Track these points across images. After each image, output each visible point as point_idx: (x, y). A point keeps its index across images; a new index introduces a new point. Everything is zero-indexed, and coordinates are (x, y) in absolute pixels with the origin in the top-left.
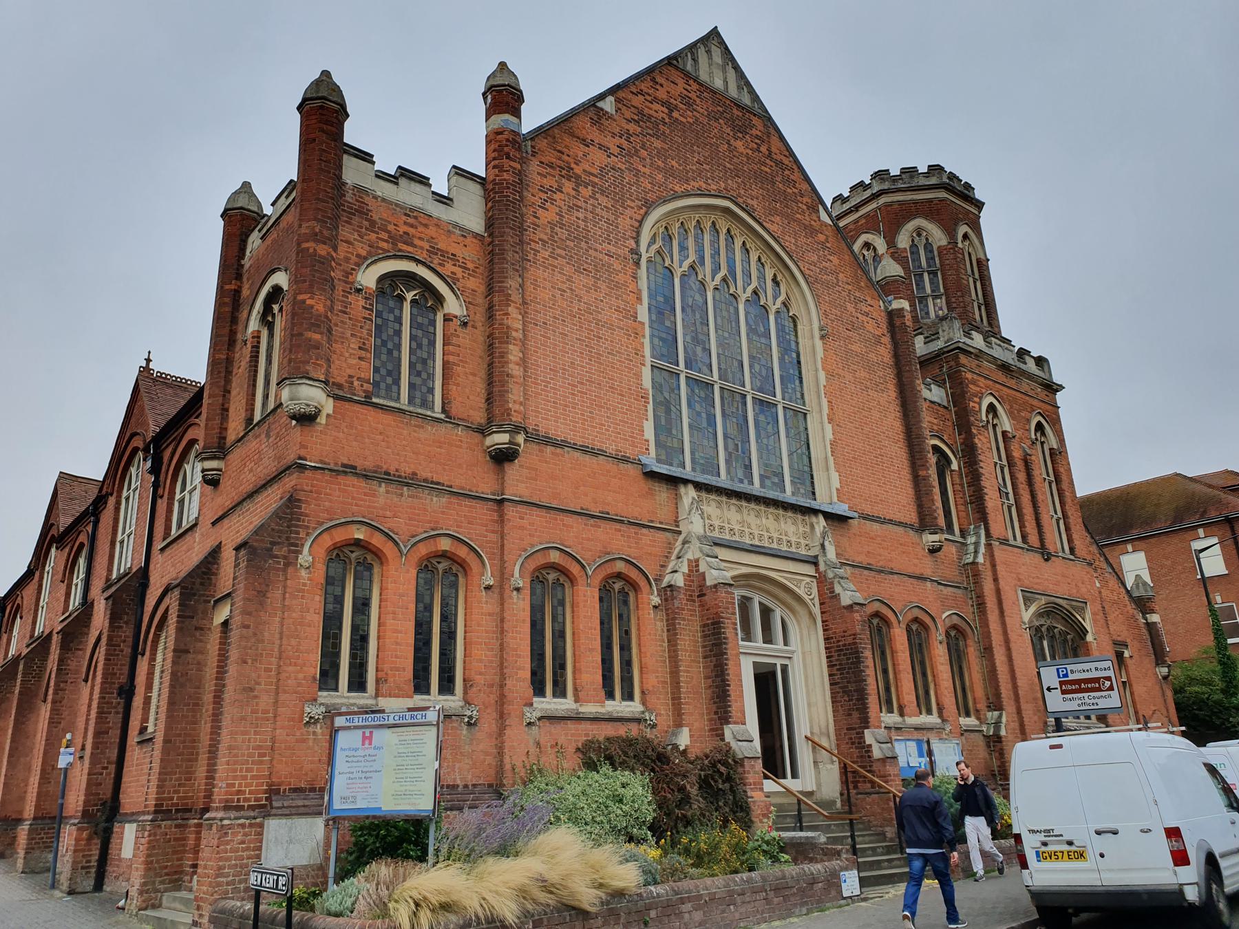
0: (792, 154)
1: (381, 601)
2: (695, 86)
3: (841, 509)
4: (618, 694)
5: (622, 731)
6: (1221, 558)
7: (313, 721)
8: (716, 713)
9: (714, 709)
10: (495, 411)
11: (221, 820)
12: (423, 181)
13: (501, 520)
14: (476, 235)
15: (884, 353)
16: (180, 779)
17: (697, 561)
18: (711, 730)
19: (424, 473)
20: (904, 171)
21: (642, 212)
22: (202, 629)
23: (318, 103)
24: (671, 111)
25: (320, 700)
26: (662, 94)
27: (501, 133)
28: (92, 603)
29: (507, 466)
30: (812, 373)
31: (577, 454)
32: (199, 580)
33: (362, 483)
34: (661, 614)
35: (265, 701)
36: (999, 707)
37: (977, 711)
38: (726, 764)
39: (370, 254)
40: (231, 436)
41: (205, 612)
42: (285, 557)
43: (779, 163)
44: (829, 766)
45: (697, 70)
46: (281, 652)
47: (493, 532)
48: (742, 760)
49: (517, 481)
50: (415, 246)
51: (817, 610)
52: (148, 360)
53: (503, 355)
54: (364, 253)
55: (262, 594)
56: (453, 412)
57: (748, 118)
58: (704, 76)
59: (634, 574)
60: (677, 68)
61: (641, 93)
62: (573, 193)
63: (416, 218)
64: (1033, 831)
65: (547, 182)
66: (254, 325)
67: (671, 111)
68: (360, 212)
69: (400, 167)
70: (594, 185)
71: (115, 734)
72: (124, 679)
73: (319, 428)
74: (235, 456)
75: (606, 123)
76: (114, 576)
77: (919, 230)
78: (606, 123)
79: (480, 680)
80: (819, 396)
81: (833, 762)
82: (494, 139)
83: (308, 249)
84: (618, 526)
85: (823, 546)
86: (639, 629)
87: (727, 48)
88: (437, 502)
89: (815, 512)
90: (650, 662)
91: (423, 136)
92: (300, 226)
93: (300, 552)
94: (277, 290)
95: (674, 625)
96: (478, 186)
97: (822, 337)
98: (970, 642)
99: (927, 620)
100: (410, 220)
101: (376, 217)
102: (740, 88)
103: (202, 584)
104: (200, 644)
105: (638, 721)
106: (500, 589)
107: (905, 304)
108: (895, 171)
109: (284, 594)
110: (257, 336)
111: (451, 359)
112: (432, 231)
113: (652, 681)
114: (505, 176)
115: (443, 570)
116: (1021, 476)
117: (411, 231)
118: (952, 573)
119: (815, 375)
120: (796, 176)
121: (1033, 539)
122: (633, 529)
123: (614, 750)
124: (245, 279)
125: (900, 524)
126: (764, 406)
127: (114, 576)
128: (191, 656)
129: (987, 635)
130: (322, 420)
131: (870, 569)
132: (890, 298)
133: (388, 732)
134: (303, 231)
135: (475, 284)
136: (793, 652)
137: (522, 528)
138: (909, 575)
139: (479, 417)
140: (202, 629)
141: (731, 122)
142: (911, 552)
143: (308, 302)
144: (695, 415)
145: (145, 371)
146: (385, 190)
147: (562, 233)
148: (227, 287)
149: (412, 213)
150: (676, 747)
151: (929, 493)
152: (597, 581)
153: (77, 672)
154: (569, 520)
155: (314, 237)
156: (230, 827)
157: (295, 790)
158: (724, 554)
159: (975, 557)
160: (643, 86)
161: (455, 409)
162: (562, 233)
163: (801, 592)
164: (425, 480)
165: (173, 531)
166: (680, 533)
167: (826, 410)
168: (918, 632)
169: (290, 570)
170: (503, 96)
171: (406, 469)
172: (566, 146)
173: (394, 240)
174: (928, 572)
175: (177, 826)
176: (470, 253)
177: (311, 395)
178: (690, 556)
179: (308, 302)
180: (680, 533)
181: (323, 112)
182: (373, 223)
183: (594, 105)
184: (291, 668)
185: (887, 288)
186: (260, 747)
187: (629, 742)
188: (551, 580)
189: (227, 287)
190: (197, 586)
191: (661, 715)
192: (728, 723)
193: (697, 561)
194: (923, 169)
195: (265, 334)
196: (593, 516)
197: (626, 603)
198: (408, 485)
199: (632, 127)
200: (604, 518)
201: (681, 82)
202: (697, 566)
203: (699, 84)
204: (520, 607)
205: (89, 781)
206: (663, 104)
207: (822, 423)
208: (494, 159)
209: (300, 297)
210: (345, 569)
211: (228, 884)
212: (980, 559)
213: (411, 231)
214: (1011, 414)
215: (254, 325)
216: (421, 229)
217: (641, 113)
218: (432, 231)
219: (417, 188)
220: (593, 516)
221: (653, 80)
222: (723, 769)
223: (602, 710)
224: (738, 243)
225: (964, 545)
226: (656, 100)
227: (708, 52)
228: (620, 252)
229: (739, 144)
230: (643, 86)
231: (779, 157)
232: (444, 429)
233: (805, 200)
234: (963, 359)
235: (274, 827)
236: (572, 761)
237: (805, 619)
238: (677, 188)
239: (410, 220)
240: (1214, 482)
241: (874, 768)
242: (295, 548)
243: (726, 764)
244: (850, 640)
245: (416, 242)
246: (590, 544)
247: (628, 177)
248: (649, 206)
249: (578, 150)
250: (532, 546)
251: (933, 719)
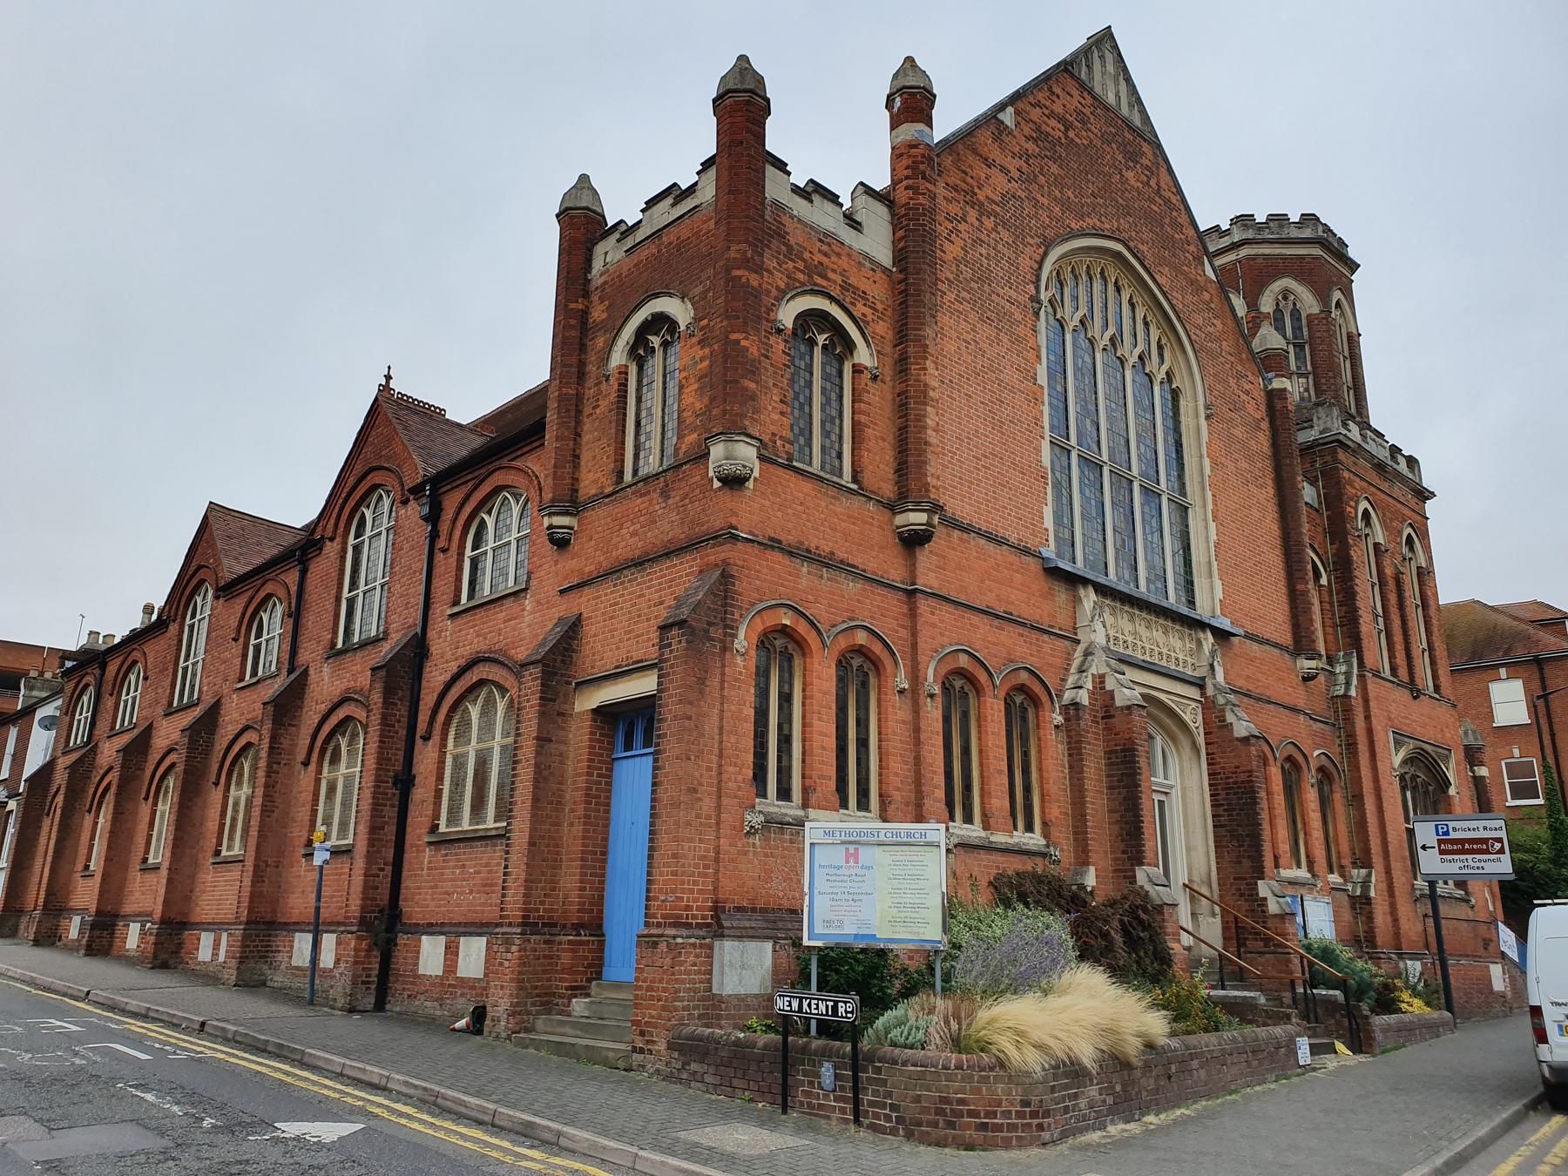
0: (1180, 192)
1: (804, 697)
2: (1089, 100)
3: (1225, 623)
4: (1020, 825)
5: (1027, 865)
6: (1524, 704)
7: (752, 832)
8: (1124, 852)
9: (1122, 847)
10: (909, 483)
11: (674, 937)
12: (833, 198)
13: (913, 614)
14: (885, 270)
15: (1262, 442)
16: (543, 888)
17: (1102, 677)
18: (1115, 871)
19: (841, 555)
20: (1272, 218)
21: (1041, 251)
22: (563, 714)
23: (745, 96)
24: (1067, 129)
25: (758, 808)
26: (1058, 108)
27: (915, 146)
28: (305, 673)
29: (917, 549)
30: (1195, 460)
31: (982, 542)
32: (560, 658)
33: (786, 560)
34: (1063, 735)
35: (708, 804)
36: (1367, 864)
37: (1342, 867)
38: (1145, 910)
39: (789, 288)
40: (587, 488)
41: (566, 695)
42: (721, 641)
43: (1167, 201)
44: (1211, 920)
45: (1091, 79)
46: (721, 751)
47: (904, 627)
48: (1161, 906)
49: (929, 570)
50: (828, 279)
51: (1201, 740)
52: (388, 377)
53: (921, 418)
54: (782, 286)
55: (702, 681)
56: (866, 483)
57: (1137, 141)
58: (1098, 89)
59: (1037, 688)
60: (1072, 76)
61: (1037, 105)
62: (977, 223)
63: (829, 245)
64: (1558, 1004)
65: (954, 209)
66: (618, 357)
67: (1067, 129)
68: (778, 234)
69: (812, 181)
70: (996, 215)
71: (390, 831)
72: (399, 767)
73: (748, 493)
74: (599, 517)
75: (1007, 139)
76: (356, 640)
77: (1286, 294)
78: (1007, 139)
79: (896, 795)
80: (1203, 489)
81: (1214, 915)
82: (897, 154)
83: (740, 277)
84: (1020, 630)
85: (1212, 666)
86: (1039, 752)
87: (1120, 55)
88: (853, 587)
90: (1053, 788)
91: (833, 147)
92: (729, 248)
93: (735, 636)
94: (660, 322)
95: (1080, 749)
96: (885, 210)
97: (1208, 417)
98: (1336, 787)
99: (1300, 759)
100: (825, 248)
101: (792, 242)
102: (1131, 105)
103: (563, 662)
104: (562, 733)
105: (1044, 855)
106: (913, 693)
108: (1261, 218)
109: (723, 681)
110: (623, 372)
111: (863, 418)
112: (844, 262)
113: (1054, 812)
114: (921, 200)
115: (859, 670)
117: (825, 260)
118: (1320, 706)
120: (1183, 219)
122: (1034, 635)
123: (1029, 887)
124: (595, 298)
125: (1276, 645)
126: (1151, 494)
127: (356, 640)
128: (553, 746)
129: (1358, 781)
130: (750, 484)
131: (1250, 696)
132: (1270, 375)
133: (878, 851)
134: (732, 254)
135: (883, 328)
136: (1171, 787)
137: (934, 625)
138: (1277, 707)
139: (888, 490)
140: (563, 714)
141: (1123, 145)
142: (1281, 676)
143: (743, 343)
144: (1085, 500)
145: (385, 389)
146: (799, 206)
147: (967, 273)
148: (572, 306)
149: (826, 237)
150: (1082, 887)
151: (1308, 611)
152: (1002, 694)
153: (291, 752)
154: (976, 619)
155: (745, 263)
156: (683, 946)
157: (739, 909)
159: (1348, 688)
160: (1040, 96)
161: (868, 479)
162: (967, 273)
163: (1187, 718)
164: (842, 562)
165: (464, 599)
166: (1078, 642)
167: (1210, 506)
168: (1292, 768)
169: (728, 655)
170: (911, 100)
171: (826, 548)
172: (970, 167)
173: (810, 270)
174: (1301, 704)
175: (546, 942)
176: (878, 291)
177: (746, 453)
178: (1093, 670)
179: (743, 343)
180: (1078, 642)
181: (742, 106)
182: (790, 248)
183: (995, 117)
184: (731, 769)
185: (1270, 362)
186: (703, 858)
187: (1038, 879)
189: (572, 306)
190: (558, 664)
191: (1063, 851)
192: (1142, 864)
193: (1102, 677)
194: (1295, 218)
195: (633, 370)
196: (998, 617)
197: (1024, 719)
198: (827, 566)
199: (1030, 146)
200: (1008, 619)
201: (1075, 92)
202: (1103, 682)
203: (1094, 98)
204: (933, 713)
205: (365, 882)
206: (1061, 119)
207: (1206, 520)
208: (907, 178)
209: (734, 336)
210: (769, 658)
211: (684, 1009)
212: (1353, 693)
213: (825, 260)
215: (618, 357)
216: (834, 259)
217: (1038, 129)
218: (844, 262)
219: (829, 206)
220: (998, 617)
221: (1050, 89)
222: (1143, 916)
223: (1010, 841)
224: (1125, 297)
225: (1333, 674)
226: (1052, 115)
227: (1102, 57)
228: (1021, 298)
229: (1130, 175)
230: (1040, 96)
231: (1168, 194)
232: (857, 501)
233: (1192, 248)
234: (1341, 455)
235: (728, 950)
236: (984, 897)
237: (1187, 750)
238: (1073, 225)
239: (825, 248)
240: (1521, 614)
241: (1269, 925)
242: (730, 630)
243: (1145, 910)
244: (1243, 777)
245: (831, 275)
246: (1000, 648)
247: (1028, 208)
248: (1048, 245)
249: (981, 171)
250: (943, 647)
251: (1302, 873)
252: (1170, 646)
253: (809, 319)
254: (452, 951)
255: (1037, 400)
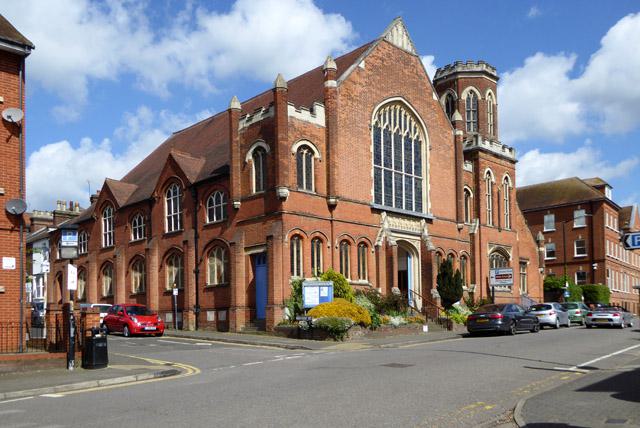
3: (430, 216)
26: (381, 56)
43: (420, 76)
51: (419, 251)
77: (471, 91)
88: (315, 220)
89: (421, 218)
107: (461, 133)
116: (496, 199)
119: (425, 165)
121: (496, 224)
135: (323, 146)
158: (393, 234)
188: (345, 243)
191: (373, 284)
214: (495, 175)
234: (480, 153)
240: (588, 182)
242: (283, 236)
246: (357, 233)
248: (375, 105)
252: (413, 226)
253: (299, 149)
254: (217, 315)
255: (370, 157)
